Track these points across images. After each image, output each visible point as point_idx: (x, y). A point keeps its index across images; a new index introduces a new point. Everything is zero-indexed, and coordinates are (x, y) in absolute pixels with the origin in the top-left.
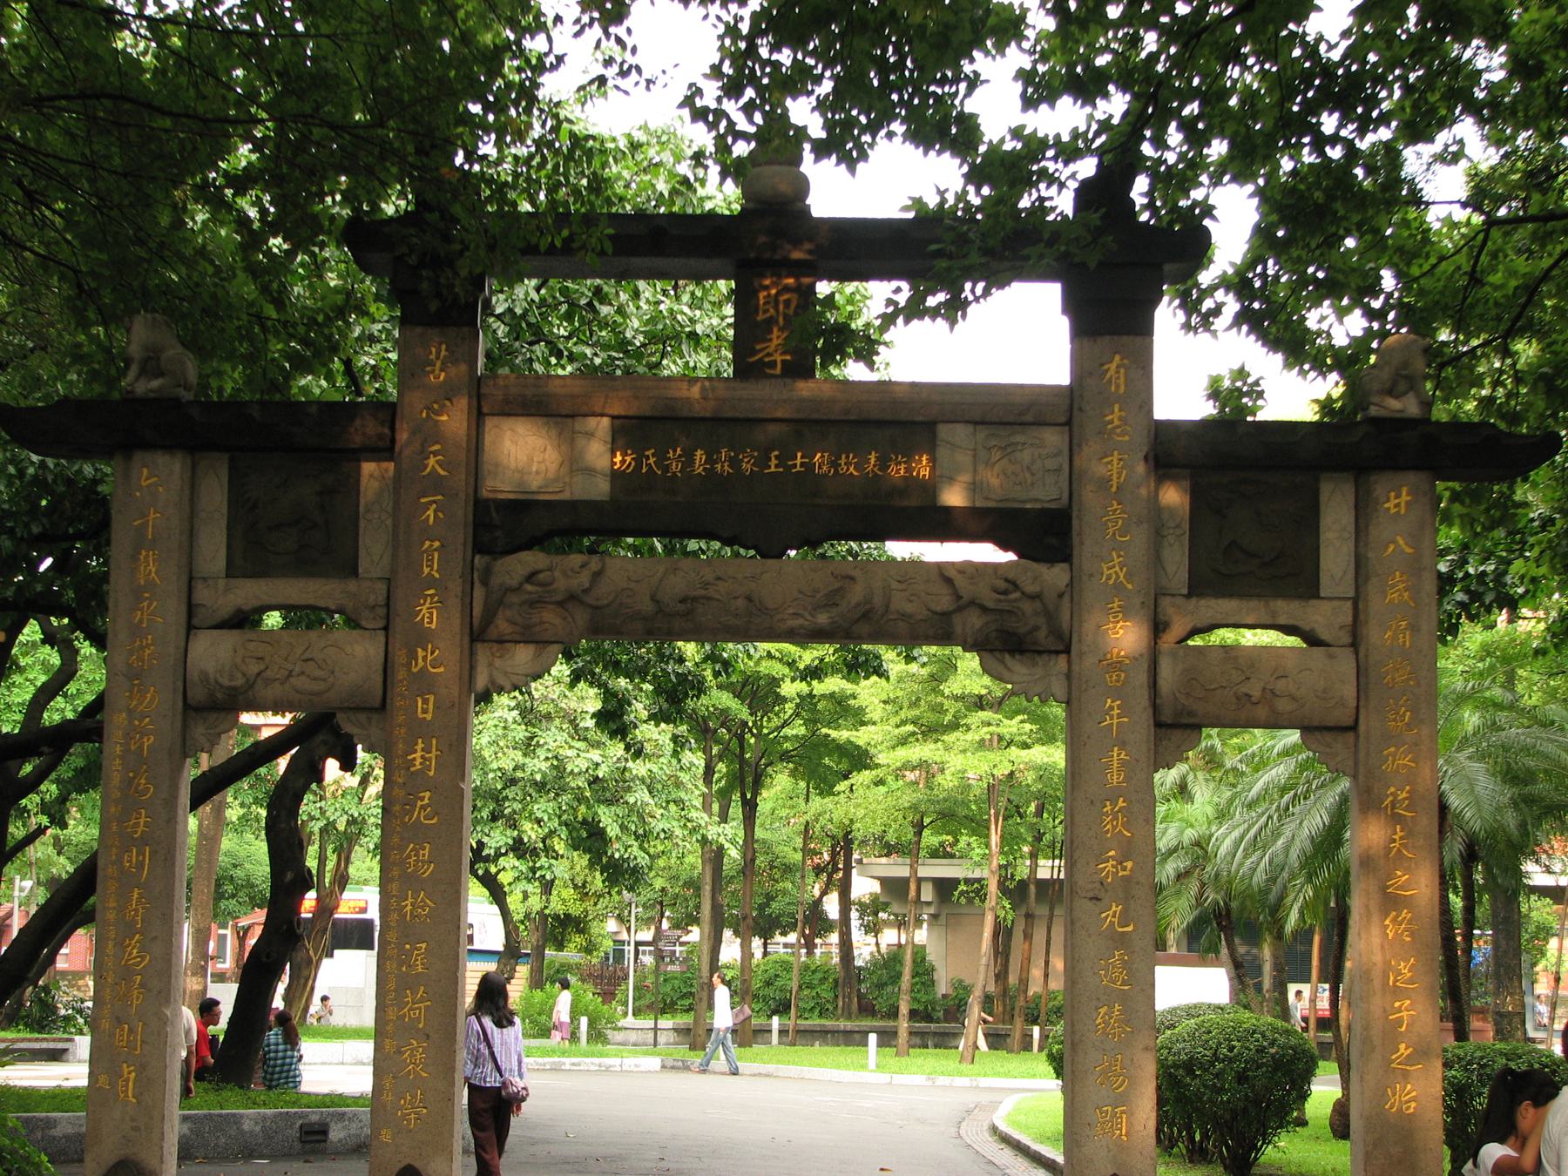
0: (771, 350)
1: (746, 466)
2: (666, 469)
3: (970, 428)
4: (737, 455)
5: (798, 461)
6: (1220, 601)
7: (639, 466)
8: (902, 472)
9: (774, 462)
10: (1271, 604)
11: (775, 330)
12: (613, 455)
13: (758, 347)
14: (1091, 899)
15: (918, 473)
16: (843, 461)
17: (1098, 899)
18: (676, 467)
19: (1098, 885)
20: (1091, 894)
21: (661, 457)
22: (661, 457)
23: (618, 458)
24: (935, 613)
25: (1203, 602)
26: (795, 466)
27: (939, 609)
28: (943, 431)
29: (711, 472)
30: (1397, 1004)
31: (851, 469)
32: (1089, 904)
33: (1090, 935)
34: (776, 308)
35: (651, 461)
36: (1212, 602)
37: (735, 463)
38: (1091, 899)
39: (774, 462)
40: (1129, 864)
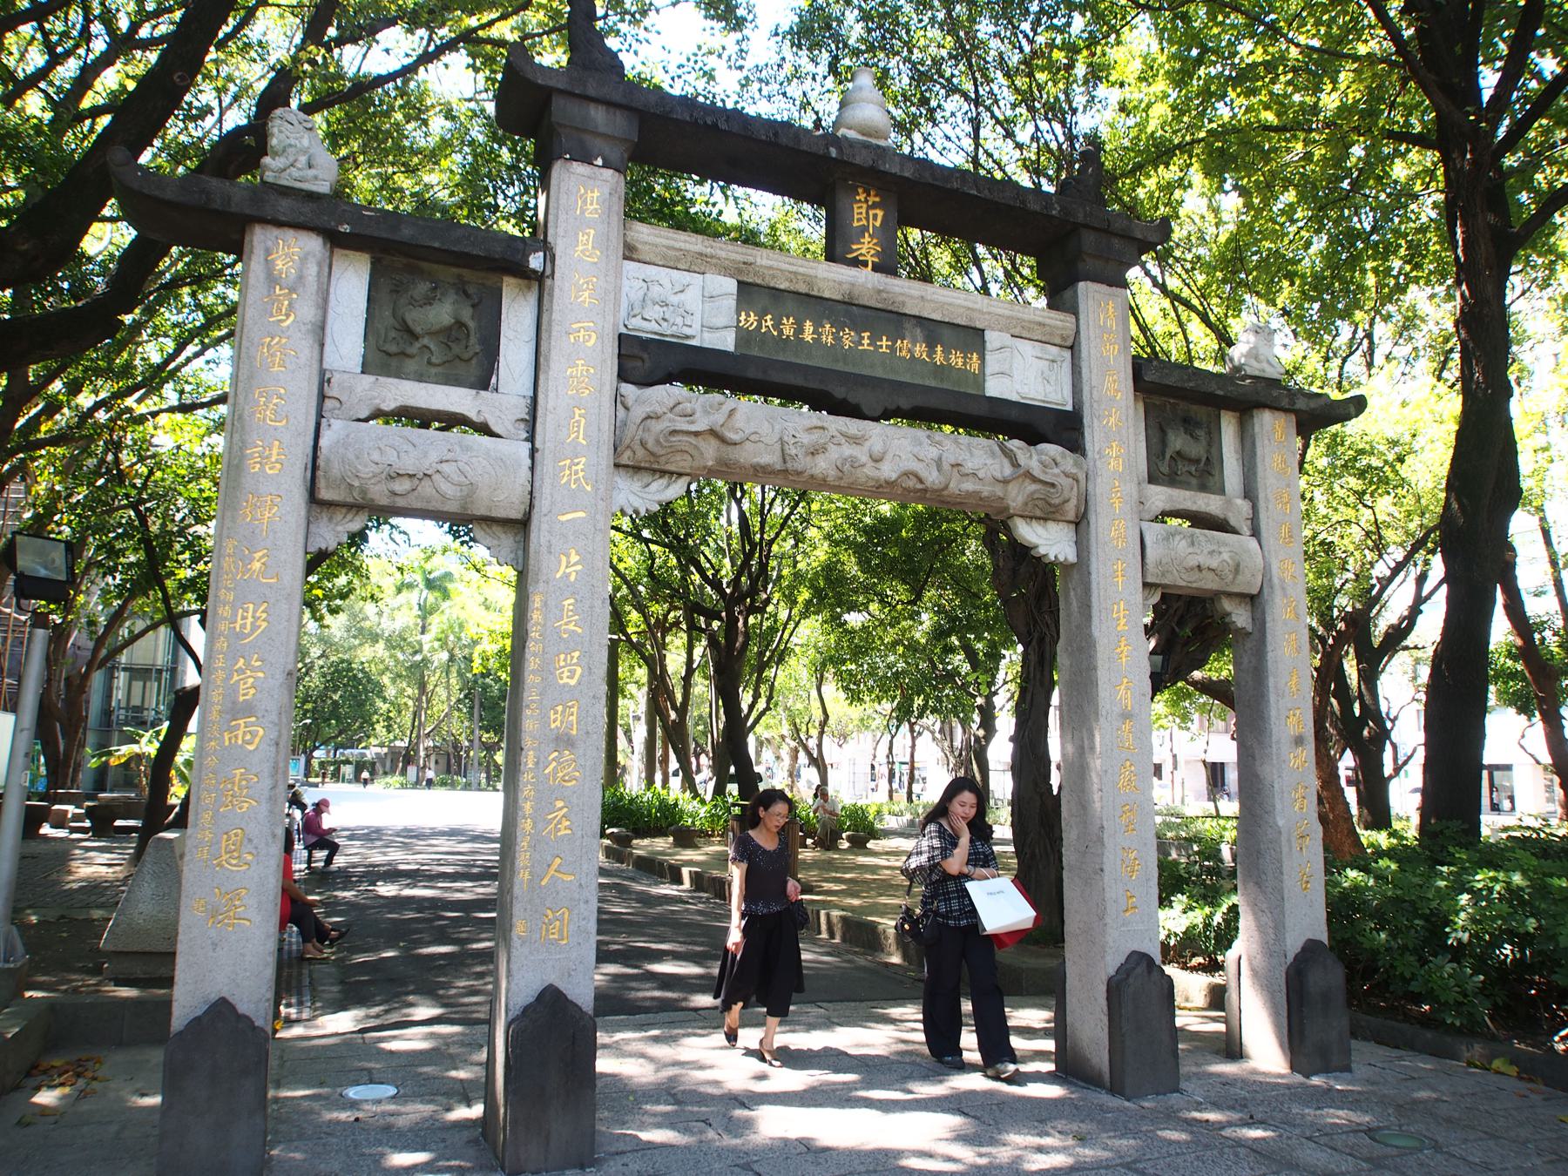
0: (863, 251)
1: (847, 344)
2: (781, 332)
5: (884, 342)
7: (760, 326)
9: (866, 341)
11: (867, 239)
12: (739, 315)
13: (854, 247)
16: (918, 348)
18: (788, 331)
21: (778, 324)
22: (778, 324)
23: (743, 317)
26: (881, 347)
29: (817, 341)
31: (924, 356)
34: (867, 219)
35: (769, 323)
37: (837, 338)
39: (866, 341)
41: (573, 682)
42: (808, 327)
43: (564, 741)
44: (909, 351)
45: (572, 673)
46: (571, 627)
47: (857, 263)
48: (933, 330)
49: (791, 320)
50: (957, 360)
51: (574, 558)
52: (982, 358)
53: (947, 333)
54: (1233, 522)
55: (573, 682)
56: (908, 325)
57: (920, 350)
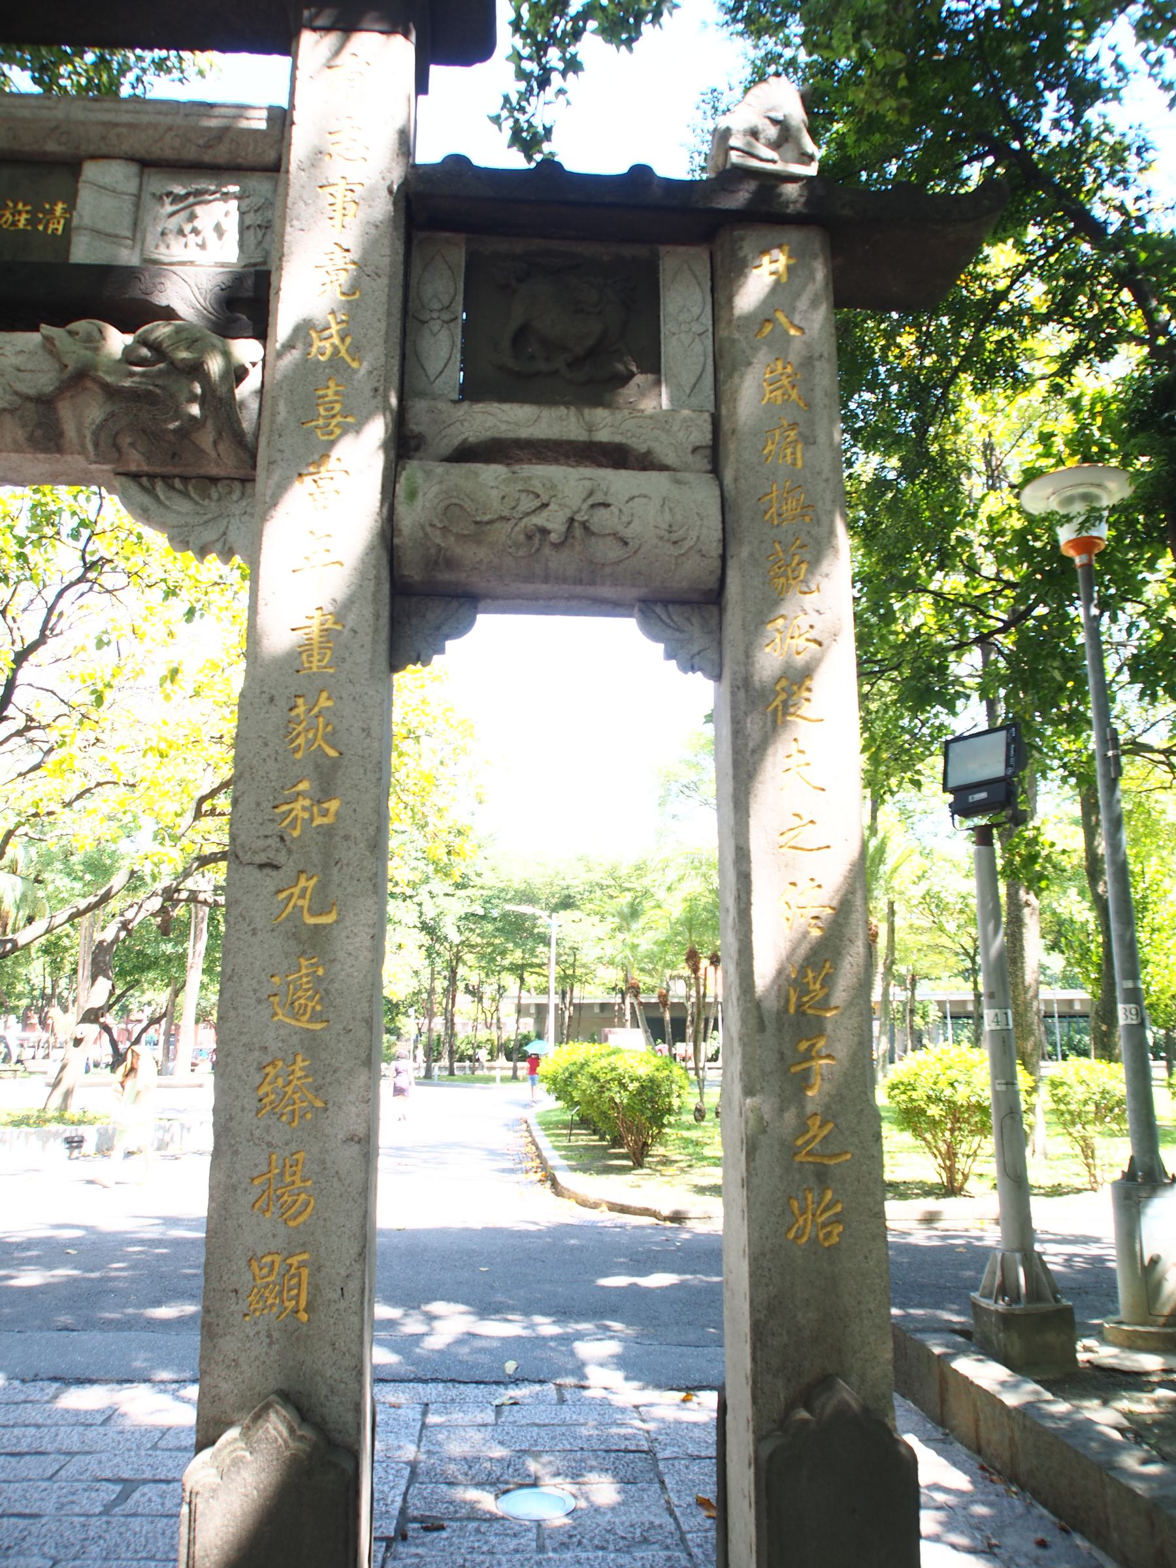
3: (133, 169)
6: (506, 407)
8: (21, 225)
10: (586, 411)
14: (262, 866)
15: (46, 227)
17: (276, 867)
19: (274, 842)
20: (261, 858)
24: (28, 398)
25: (479, 407)
27: (32, 392)
28: (90, 170)
30: (803, 1046)
32: (257, 874)
33: (254, 932)
36: (494, 407)
38: (262, 866)
40: (333, 805)
52: (71, 207)
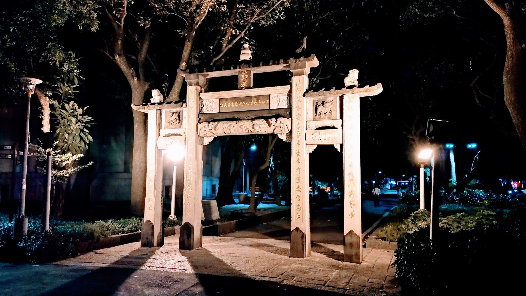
0: (244, 85)
4: (238, 103)
18: (229, 106)
37: (238, 105)
39: (244, 104)
41: (191, 174)
42: (233, 104)
43: (190, 184)
44: (253, 103)
45: (191, 173)
46: (191, 165)
47: (242, 88)
48: (258, 98)
49: (229, 103)
50: (263, 102)
51: (191, 154)
53: (261, 97)
54: (336, 126)
55: (191, 174)
56: (253, 98)
57: (256, 103)
